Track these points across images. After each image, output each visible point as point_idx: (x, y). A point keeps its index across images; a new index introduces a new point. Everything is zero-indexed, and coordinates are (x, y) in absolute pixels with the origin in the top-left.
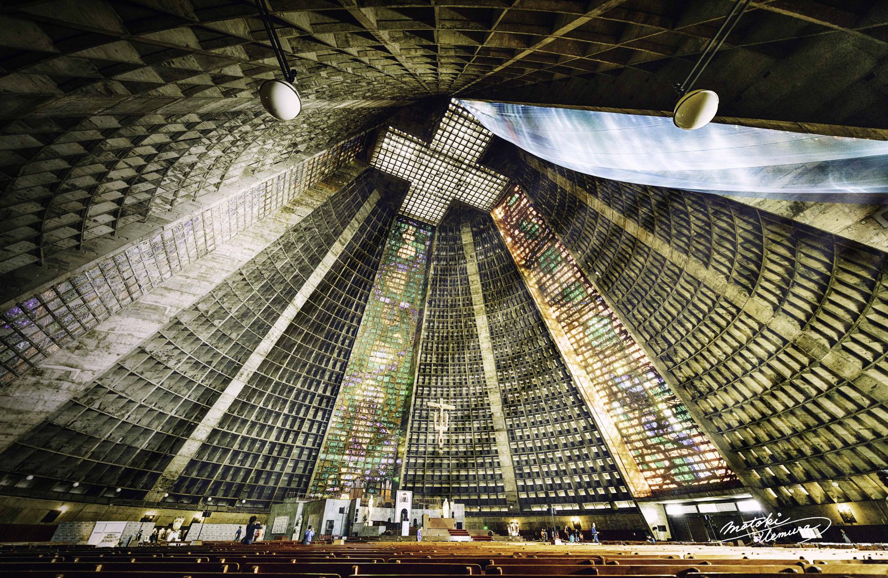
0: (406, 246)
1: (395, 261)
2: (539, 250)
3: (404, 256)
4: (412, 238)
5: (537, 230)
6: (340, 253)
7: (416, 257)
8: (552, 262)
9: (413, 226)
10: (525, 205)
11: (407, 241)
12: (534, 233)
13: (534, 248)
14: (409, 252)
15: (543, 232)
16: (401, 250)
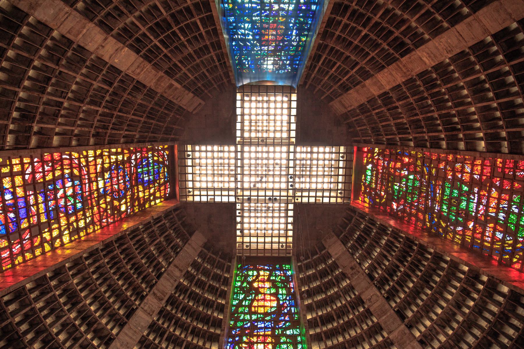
0: (260, 297)
1: (250, 321)
2: (434, 200)
3: (261, 310)
4: (267, 285)
5: (414, 179)
6: (157, 311)
7: (280, 307)
8: (460, 202)
9: (265, 270)
10: (384, 168)
11: (262, 290)
12: (414, 187)
13: (426, 204)
14: (268, 304)
15: (422, 176)
16: (255, 304)
